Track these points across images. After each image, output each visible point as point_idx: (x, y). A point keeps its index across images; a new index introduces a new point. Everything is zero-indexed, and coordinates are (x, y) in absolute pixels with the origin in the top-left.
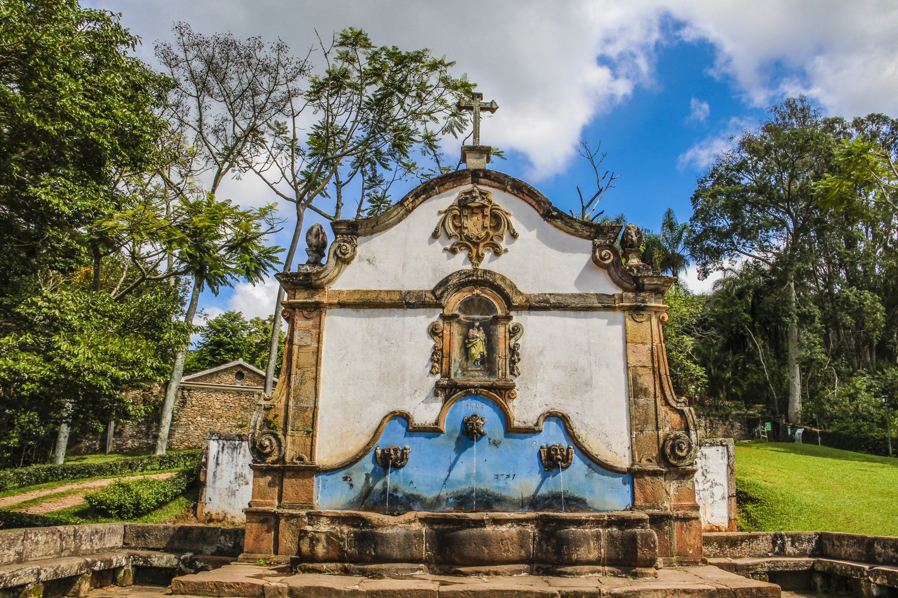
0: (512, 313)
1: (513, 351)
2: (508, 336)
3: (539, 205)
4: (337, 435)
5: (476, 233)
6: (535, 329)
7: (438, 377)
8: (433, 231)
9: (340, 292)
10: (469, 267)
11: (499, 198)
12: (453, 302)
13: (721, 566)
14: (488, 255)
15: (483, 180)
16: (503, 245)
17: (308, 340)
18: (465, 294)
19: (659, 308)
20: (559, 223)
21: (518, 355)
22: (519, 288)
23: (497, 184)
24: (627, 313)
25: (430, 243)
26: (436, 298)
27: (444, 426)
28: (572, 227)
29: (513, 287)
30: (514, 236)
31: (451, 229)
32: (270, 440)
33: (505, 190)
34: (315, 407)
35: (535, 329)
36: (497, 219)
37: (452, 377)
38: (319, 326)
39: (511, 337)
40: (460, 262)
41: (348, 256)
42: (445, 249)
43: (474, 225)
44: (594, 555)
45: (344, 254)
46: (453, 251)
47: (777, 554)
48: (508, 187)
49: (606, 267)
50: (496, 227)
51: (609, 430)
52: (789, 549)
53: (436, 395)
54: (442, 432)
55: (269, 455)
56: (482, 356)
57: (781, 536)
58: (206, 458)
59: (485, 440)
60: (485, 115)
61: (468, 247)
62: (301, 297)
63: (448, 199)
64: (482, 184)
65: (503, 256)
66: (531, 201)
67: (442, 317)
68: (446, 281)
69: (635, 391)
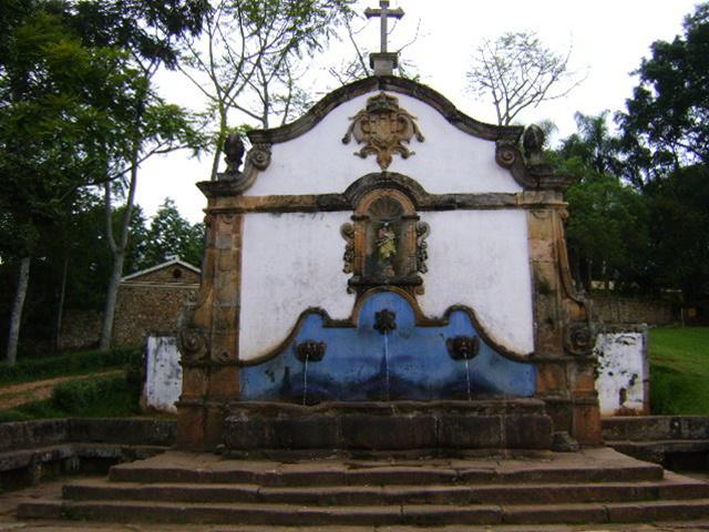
0: (420, 214)
2: (415, 235)
3: (444, 109)
4: (260, 328)
5: (384, 137)
6: (442, 228)
7: (351, 275)
8: (343, 137)
9: (258, 198)
10: (377, 169)
11: (406, 103)
12: (364, 205)
13: (618, 449)
14: (396, 158)
15: (389, 86)
18: (375, 195)
19: (559, 205)
20: (462, 125)
21: (425, 252)
24: (528, 211)
27: (357, 322)
28: (475, 129)
29: (419, 188)
30: (421, 139)
31: (361, 135)
33: (411, 95)
35: (442, 228)
36: (404, 122)
37: (364, 275)
38: (237, 230)
39: (418, 236)
40: (370, 166)
41: (264, 163)
42: (356, 154)
43: (382, 130)
44: (494, 440)
45: (261, 162)
46: (363, 155)
47: (674, 437)
50: (402, 131)
51: (513, 324)
52: (686, 432)
53: (349, 292)
55: (195, 352)
56: (392, 254)
57: (678, 420)
58: (146, 355)
59: (395, 333)
60: (391, 21)
61: (376, 151)
62: (222, 204)
63: (358, 104)
64: (388, 90)
65: (411, 158)
66: (435, 104)
67: (353, 218)
68: (356, 184)
69: (540, 289)
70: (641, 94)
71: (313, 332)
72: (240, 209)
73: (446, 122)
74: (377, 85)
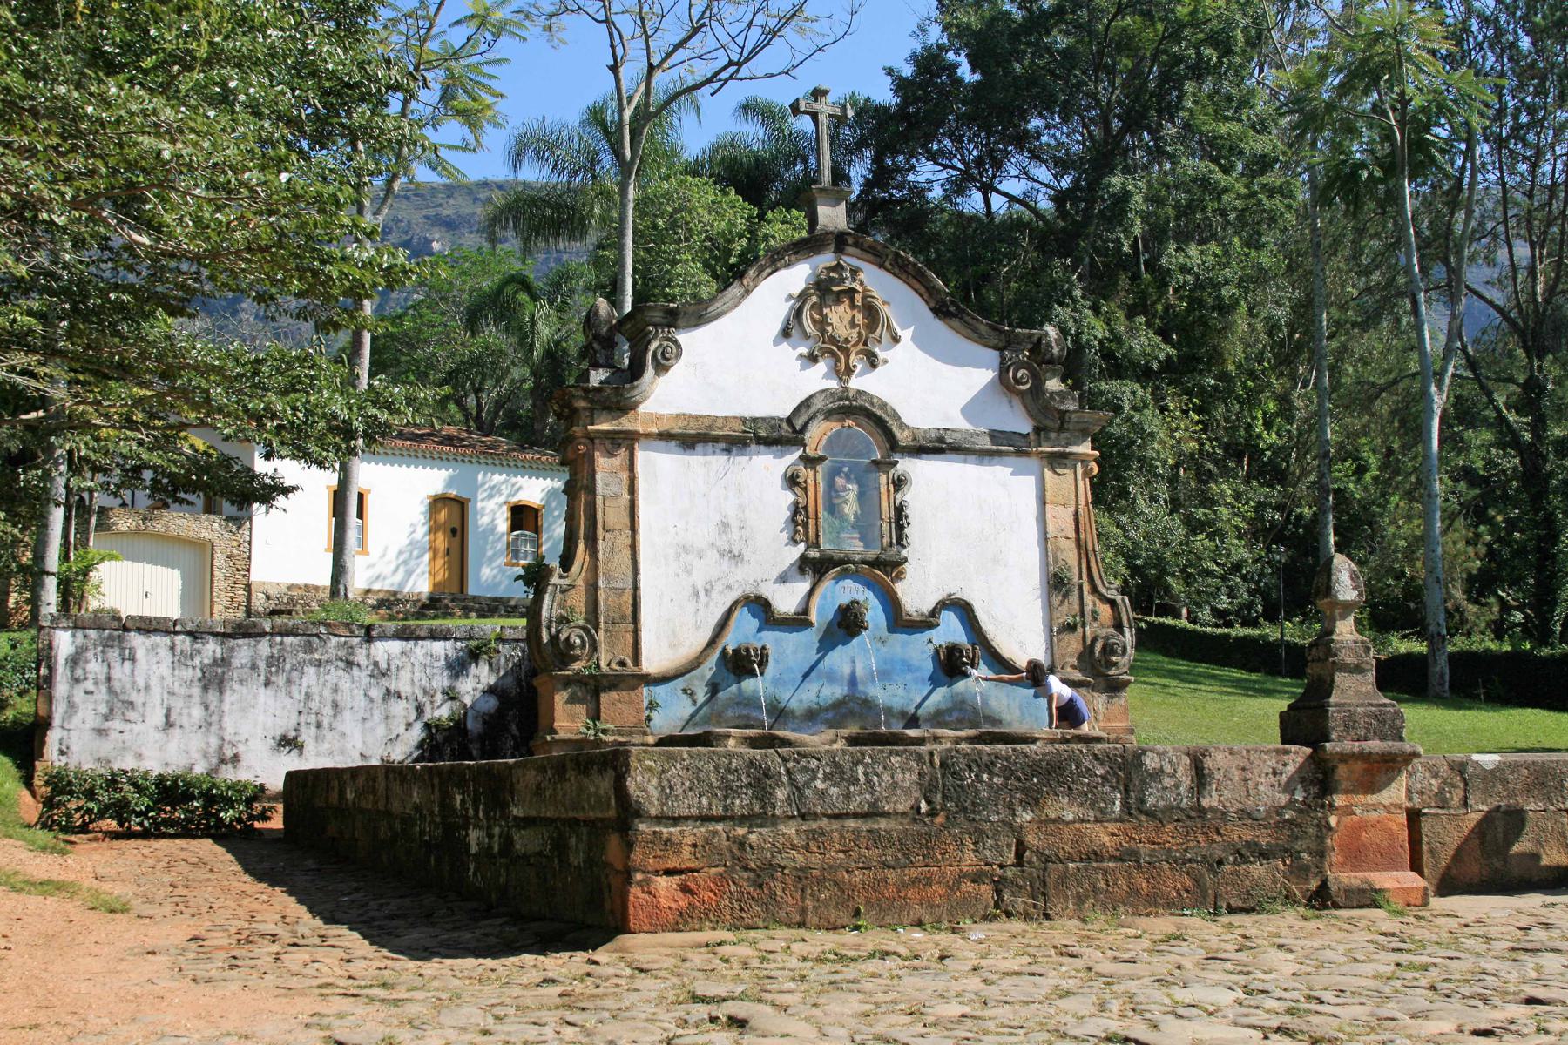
0: (896, 457)
1: (900, 511)
3: (930, 295)
7: (802, 546)
9: (659, 417)
10: (833, 384)
15: (850, 250)
16: (881, 355)
17: (615, 489)
20: (956, 323)
22: (904, 419)
23: (870, 257)
25: (776, 343)
26: (794, 431)
29: (896, 417)
32: (581, 637)
33: (881, 266)
34: (636, 588)
36: (871, 313)
39: (896, 491)
43: (840, 318)
46: (812, 359)
48: (887, 264)
49: (1021, 394)
54: (810, 624)
58: (51, 668)
65: (880, 369)
66: (917, 286)
68: (806, 403)
70: (930, 63)
71: (744, 631)
72: (637, 433)
73: (930, 314)
74: (832, 247)
